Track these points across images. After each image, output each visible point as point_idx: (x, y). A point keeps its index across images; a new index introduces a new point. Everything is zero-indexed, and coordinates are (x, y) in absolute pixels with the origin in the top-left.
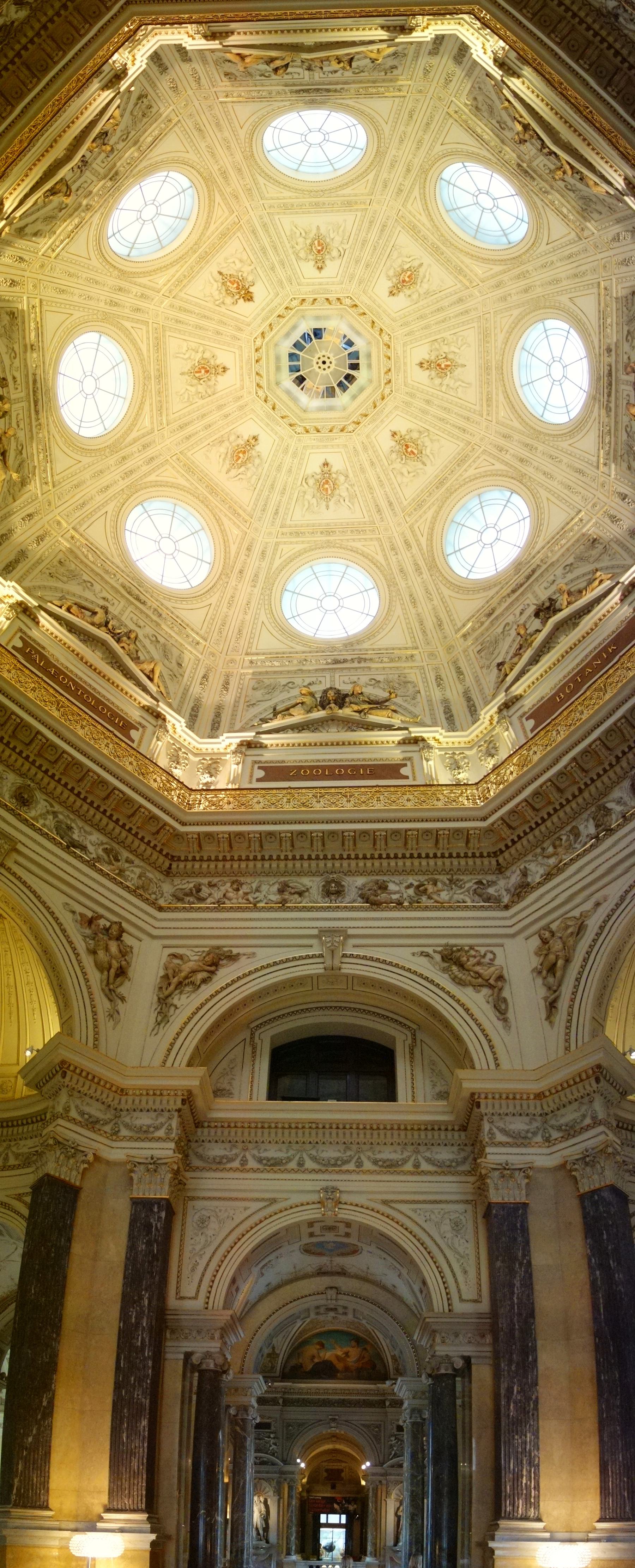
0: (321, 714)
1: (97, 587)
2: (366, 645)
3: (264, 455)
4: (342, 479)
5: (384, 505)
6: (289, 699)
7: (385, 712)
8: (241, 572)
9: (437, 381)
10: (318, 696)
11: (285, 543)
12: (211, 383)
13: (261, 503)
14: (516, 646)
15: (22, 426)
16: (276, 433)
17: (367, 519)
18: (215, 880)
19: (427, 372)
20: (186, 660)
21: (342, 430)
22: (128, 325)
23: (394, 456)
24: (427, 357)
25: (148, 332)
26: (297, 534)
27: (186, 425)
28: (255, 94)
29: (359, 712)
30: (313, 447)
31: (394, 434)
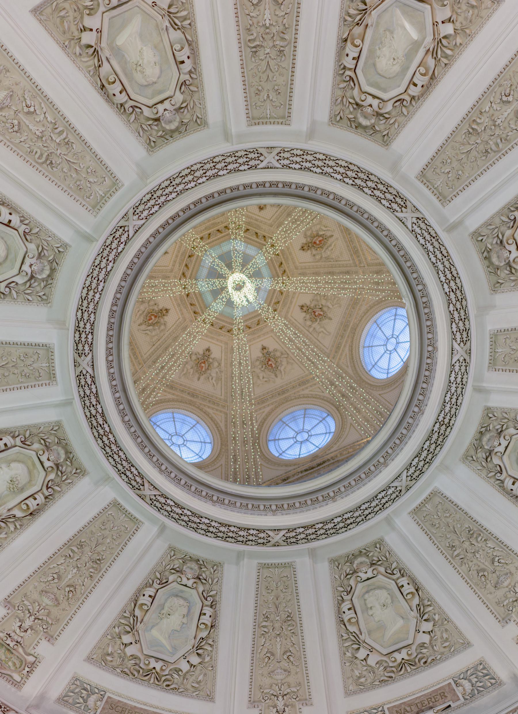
3: (169, 325)
4: (216, 364)
9: (309, 323)
16: (182, 314)
17: (223, 397)
19: (304, 314)
24: (308, 303)
31: (264, 348)
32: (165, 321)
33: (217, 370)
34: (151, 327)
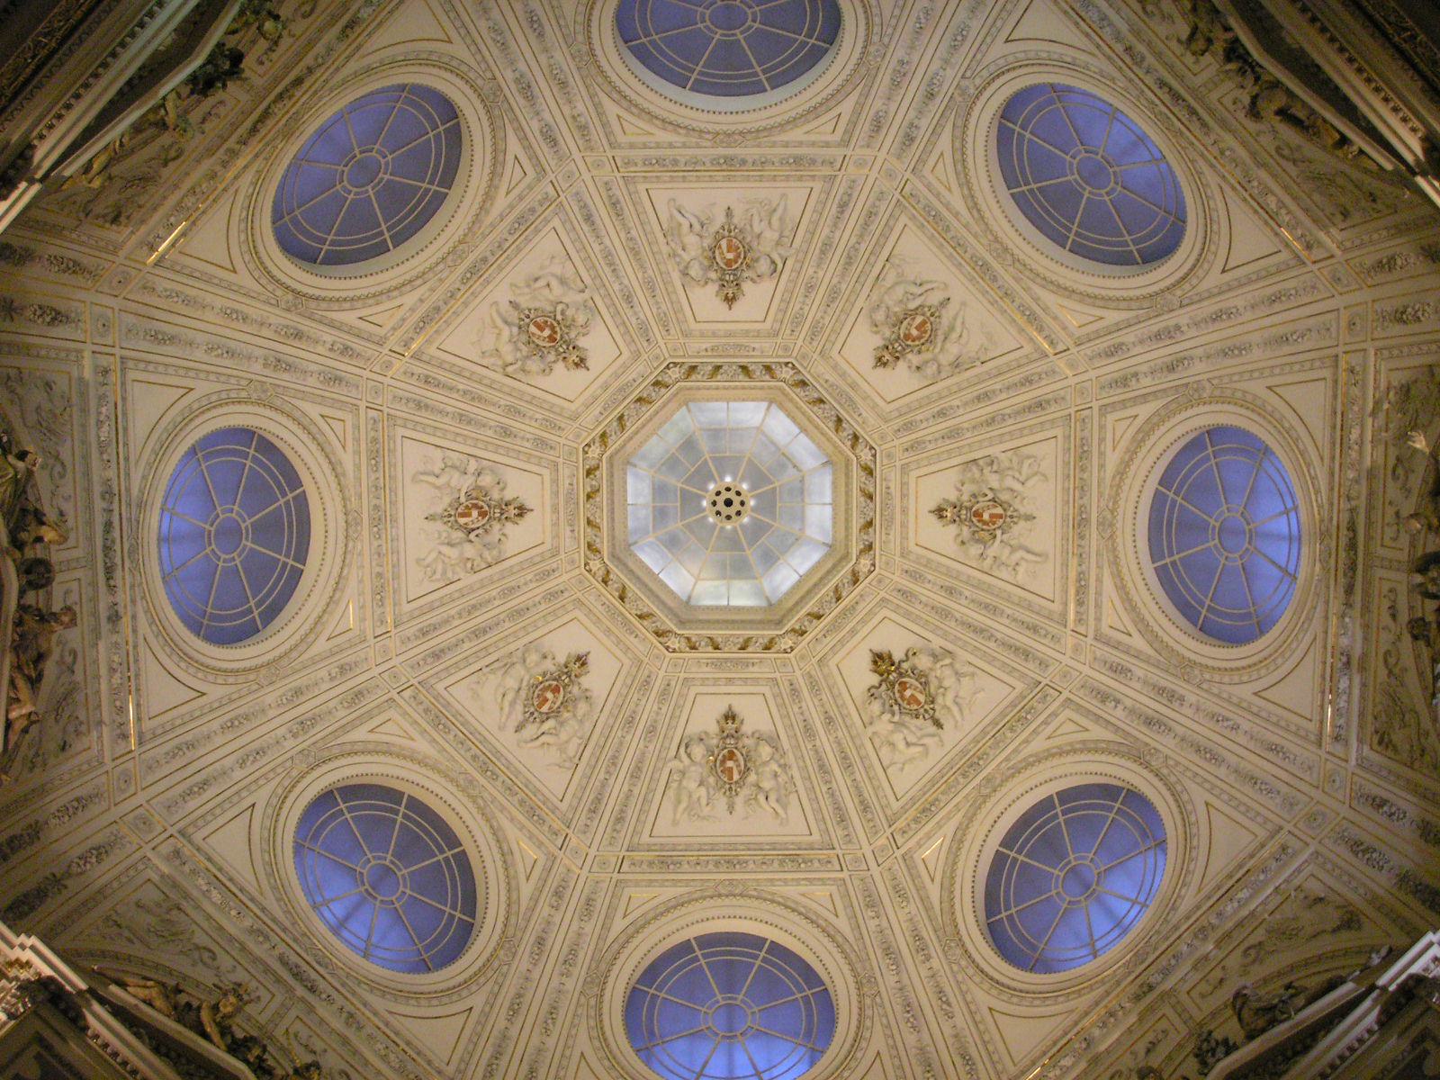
3: (863, 328)
4: (695, 271)
9: (486, 480)
11: (827, 145)
12: (969, 489)
13: (877, 226)
16: (835, 367)
19: (509, 495)
23: (581, 319)
24: (509, 528)
25: (1098, 619)
26: (798, 160)
30: (758, 334)
32: (876, 333)
33: (686, 257)
34: (912, 305)
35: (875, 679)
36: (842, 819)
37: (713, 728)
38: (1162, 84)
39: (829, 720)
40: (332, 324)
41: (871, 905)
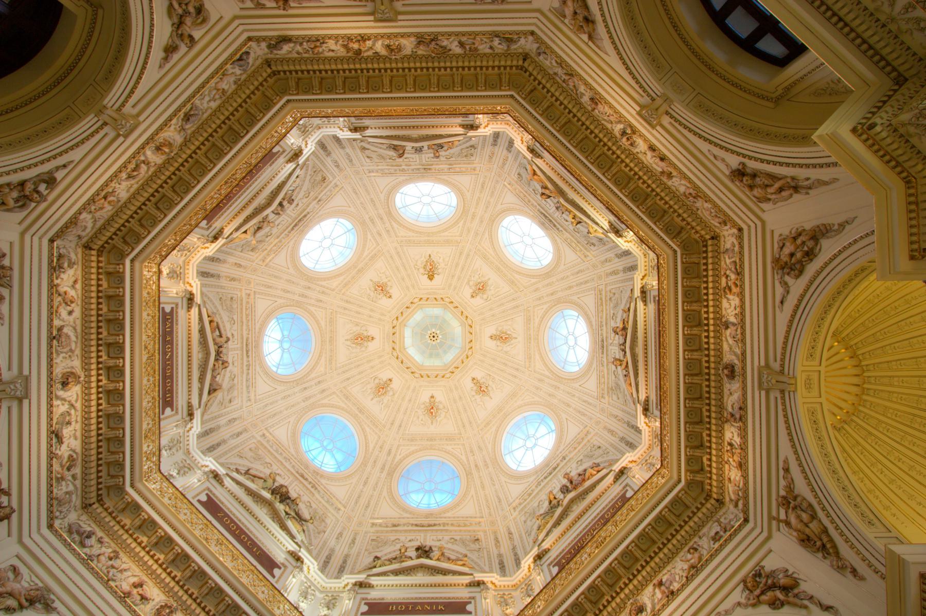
0: (267, 495)
1: (235, 327)
2: (323, 481)
4: (391, 393)
5: (397, 423)
6: (261, 472)
7: (298, 526)
8: (305, 389)
9: (473, 393)
10: (276, 484)
12: (380, 297)
14: (393, 555)
15: (279, 227)
18: (106, 539)
20: (235, 402)
21: (412, 373)
22: (369, 237)
23: (422, 406)
24: (479, 378)
26: (347, 398)
27: (349, 302)
28: (522, 195)
29: (287, 513)
31: (432, 397)
35: (435, 276)
36: (468, 255)
37: (478, 297)
38: (248, 356)
39: (453, 276)
40: (468, 460)
41: (477, 234)
